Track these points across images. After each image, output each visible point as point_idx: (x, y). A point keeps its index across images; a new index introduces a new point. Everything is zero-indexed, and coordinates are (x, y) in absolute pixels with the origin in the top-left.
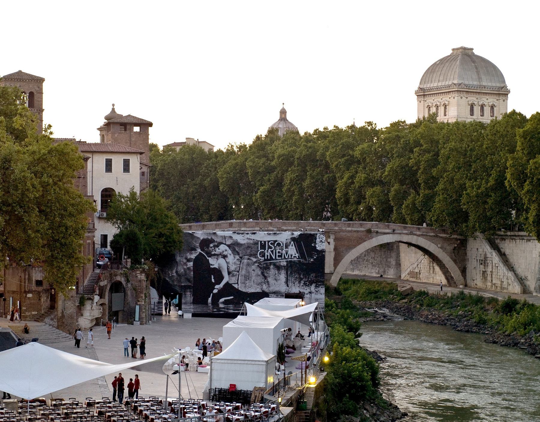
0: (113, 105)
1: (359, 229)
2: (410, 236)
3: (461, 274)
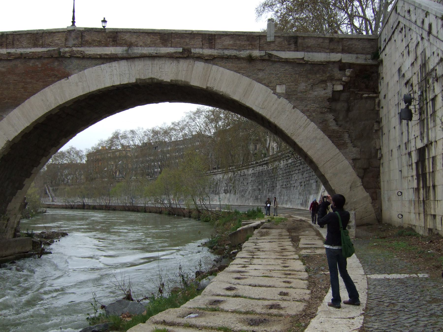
1: (29, 50)
2: (183, 64)
3: (359, 182)
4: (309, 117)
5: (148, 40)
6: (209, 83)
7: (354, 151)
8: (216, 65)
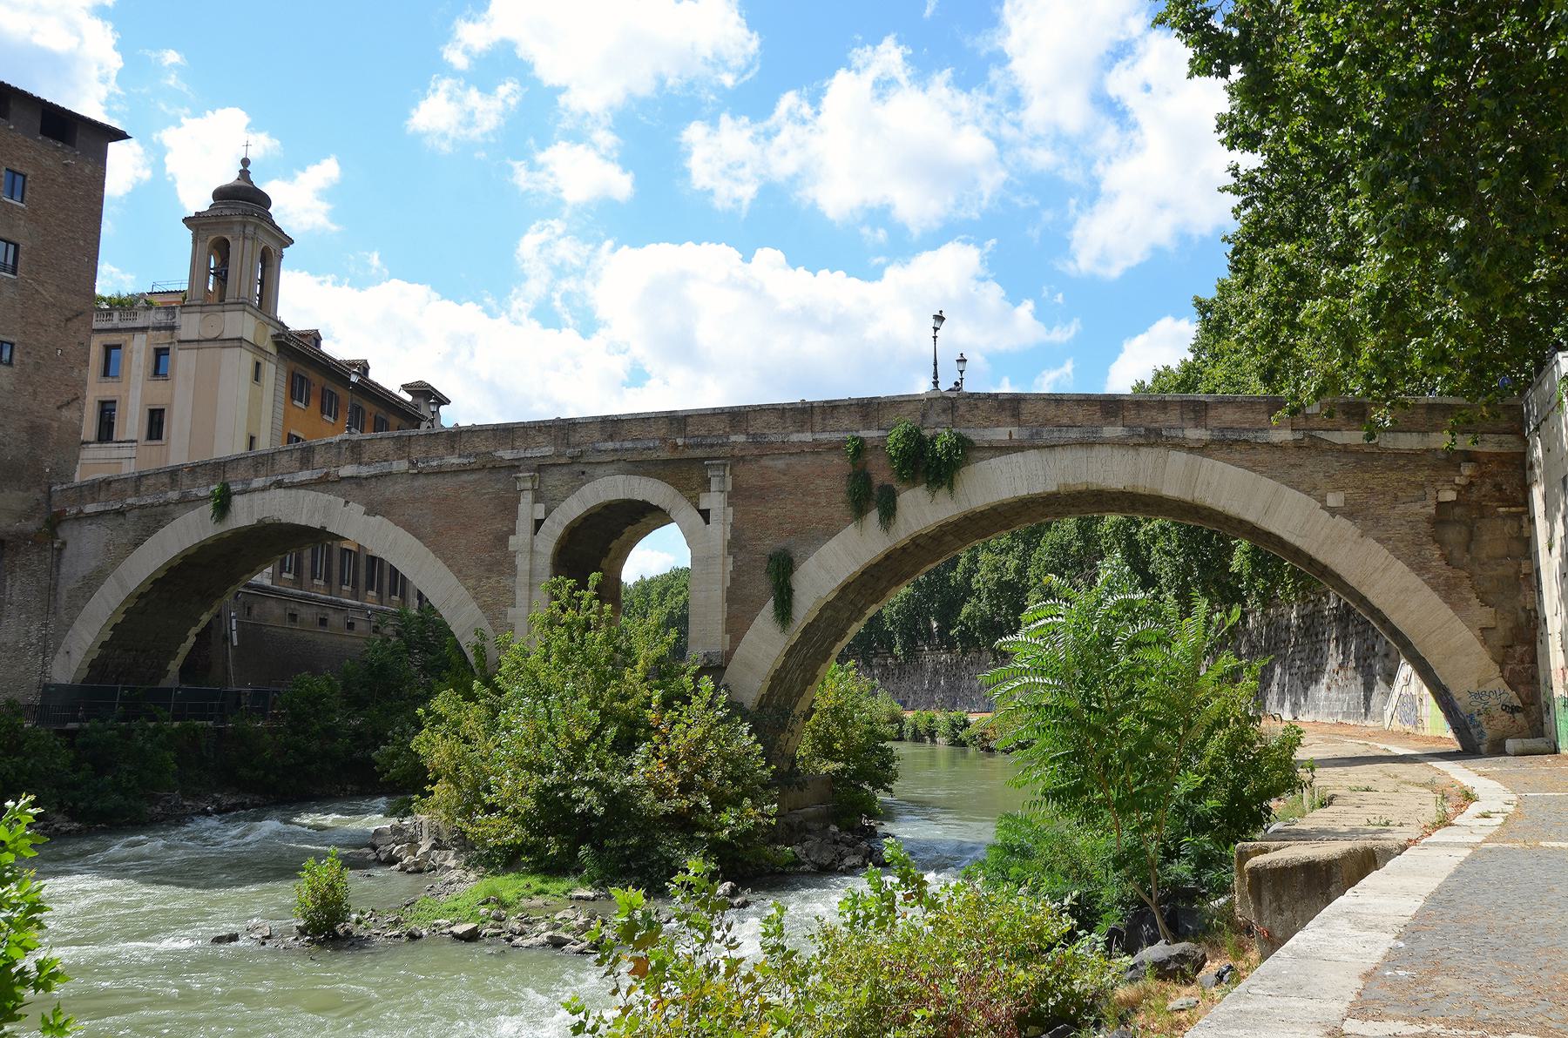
0: (245, 162)
2: (1148, 456)
4: (1392, 551)
5: (1080, 414)
6: (1197, 490)
7: (1484, 616)
8: (1209, 456)
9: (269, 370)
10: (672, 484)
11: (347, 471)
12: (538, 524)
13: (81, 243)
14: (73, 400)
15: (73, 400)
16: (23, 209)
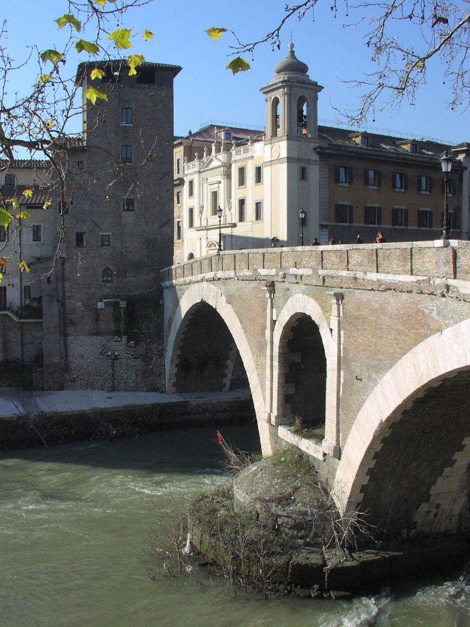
0: (292, 46)
9: (314, 172)
10: (320, 305)
11: (220, 274)
12: (274, 322)
13: (164, 135)
14: (167, 222)
15: (167, 222)
16: (131, 127)
